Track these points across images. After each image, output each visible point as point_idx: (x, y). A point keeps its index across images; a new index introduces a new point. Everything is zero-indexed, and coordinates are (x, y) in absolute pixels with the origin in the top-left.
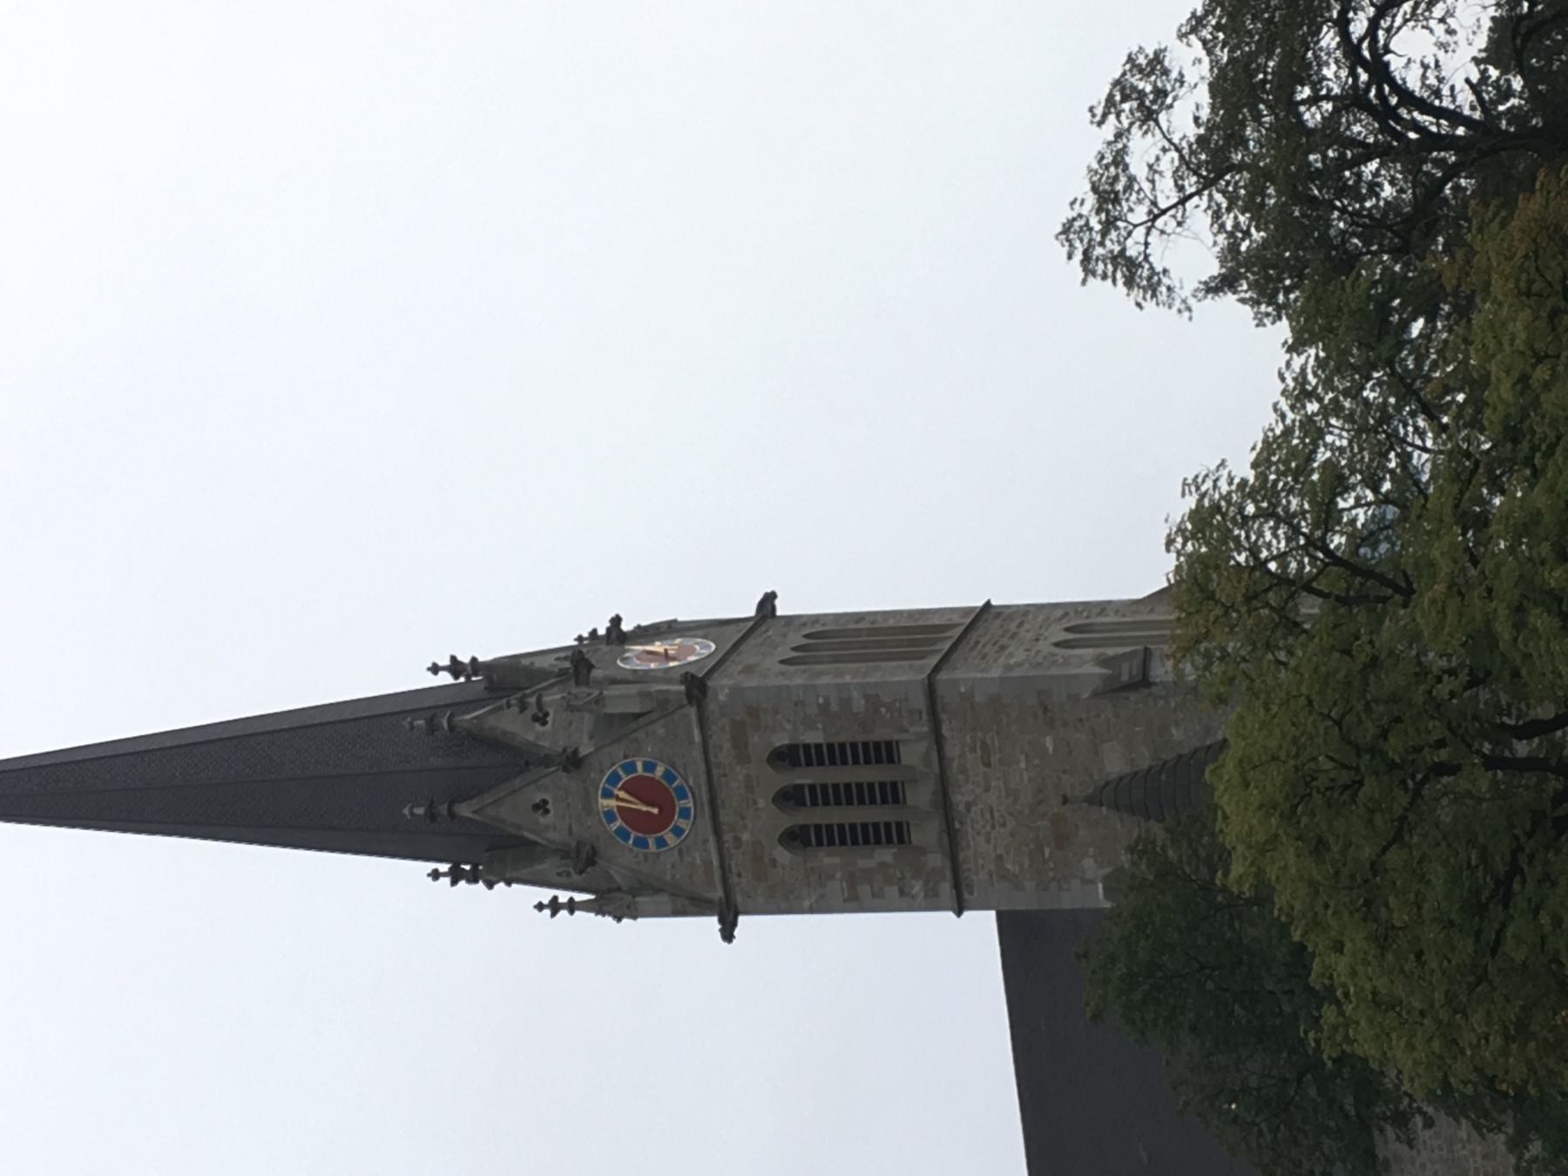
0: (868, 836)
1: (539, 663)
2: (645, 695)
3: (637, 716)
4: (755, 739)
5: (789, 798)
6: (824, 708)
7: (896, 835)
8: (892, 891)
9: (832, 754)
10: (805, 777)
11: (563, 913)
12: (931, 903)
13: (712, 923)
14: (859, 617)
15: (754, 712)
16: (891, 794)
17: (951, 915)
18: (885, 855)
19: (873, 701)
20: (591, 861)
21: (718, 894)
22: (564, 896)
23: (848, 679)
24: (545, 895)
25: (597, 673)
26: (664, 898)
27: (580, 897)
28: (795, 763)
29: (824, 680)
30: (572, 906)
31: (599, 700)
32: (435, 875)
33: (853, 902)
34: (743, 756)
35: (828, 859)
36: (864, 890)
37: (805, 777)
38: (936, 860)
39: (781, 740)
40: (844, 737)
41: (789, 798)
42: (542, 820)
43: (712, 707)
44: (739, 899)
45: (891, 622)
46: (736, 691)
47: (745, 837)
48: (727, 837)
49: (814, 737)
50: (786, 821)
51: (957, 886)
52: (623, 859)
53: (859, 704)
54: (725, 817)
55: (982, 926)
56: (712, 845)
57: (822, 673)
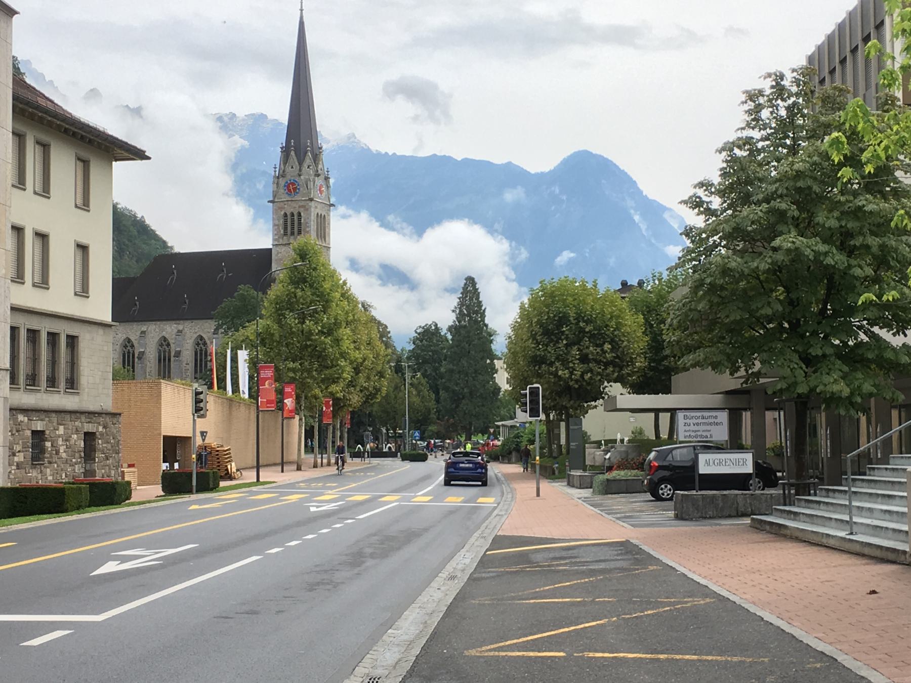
0: (285, 229)
1: (320, 166)
2: (311, 189)
3: (307, 187)
4: (302, 209)
5: (292, 215)
6: (307, 223)
7: (285, 234)
8: (276, 232)
9: (300, 224)
10: (296, 218)
11: (274, 169)
12: (274, 240)
13: (271, 199)
14: (329, 224)
15: (307, 210)
16: (292, 234)
17: (271, 243)
18: (282, 232)
19: (308, 232)
20: (282, 176)
21: (276, 200)
22: (277, 170)
23: (312, 227)
24: (278, 166)
25: (316, 178)
26: (276, 189)
27: (277, 173)
28: (299, 216)
29: (312, 223)
30: (275, 171)
31: (310, 180)
32: (282, 144)
33: (274, 225)
34: (300, 207)
35: (282, 221)
36: (276, 227)
37: (296, 218)
38: (281, 242)
39: (302, 214)
40: (302, 226)
41: (292, 215)
42: (290, 167)
43: (308, 202)
44: (276, 204)
45: (327, 230)
46: (311, 207)
47: (286, 206)
48: (286, 203)
49: (302, 220)
50: (288, 214)
51: (276, 245)
52: (282, 182)
53: (308, 229)
54: (290, 202)
55: (271, 247)
56: (285, 200)
57: (314, 221)
